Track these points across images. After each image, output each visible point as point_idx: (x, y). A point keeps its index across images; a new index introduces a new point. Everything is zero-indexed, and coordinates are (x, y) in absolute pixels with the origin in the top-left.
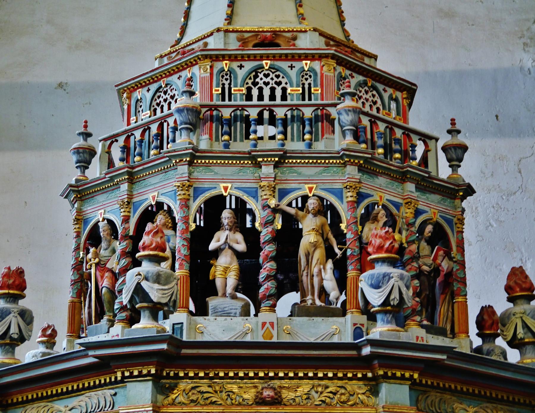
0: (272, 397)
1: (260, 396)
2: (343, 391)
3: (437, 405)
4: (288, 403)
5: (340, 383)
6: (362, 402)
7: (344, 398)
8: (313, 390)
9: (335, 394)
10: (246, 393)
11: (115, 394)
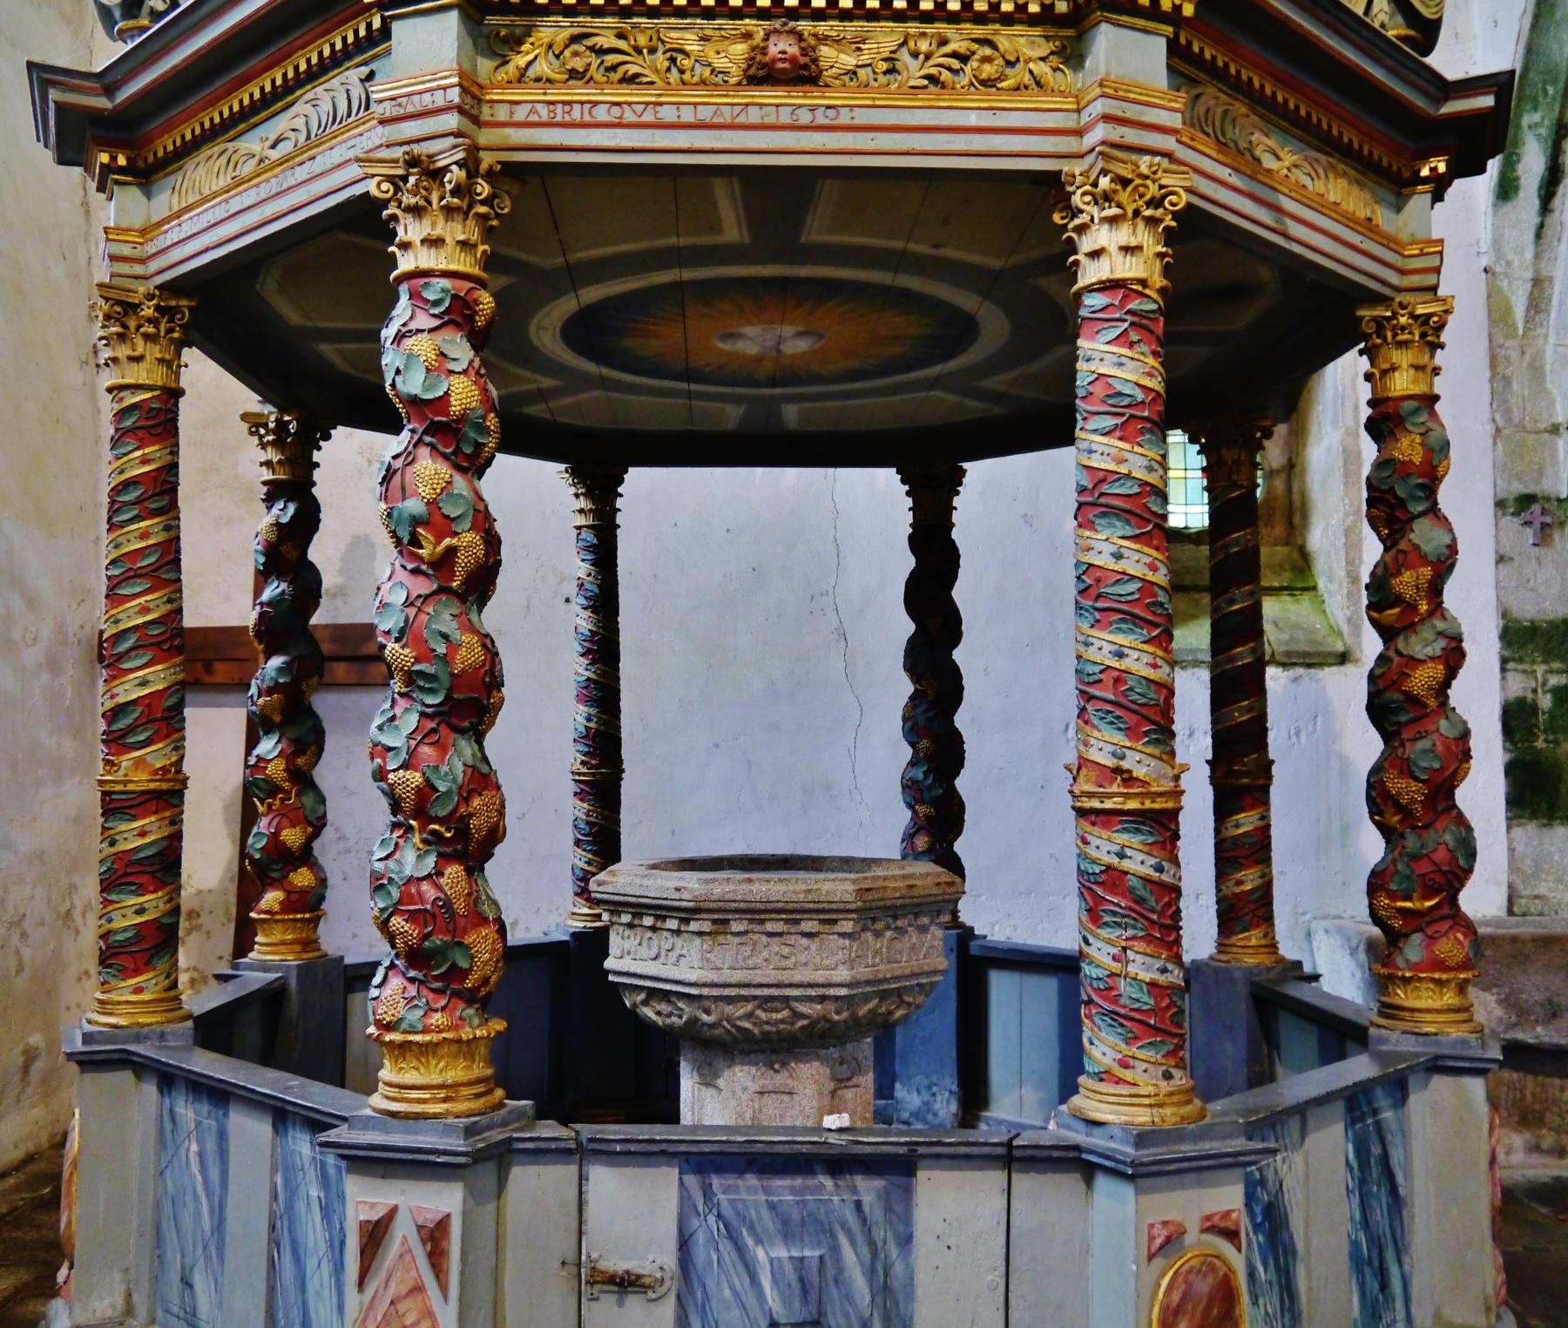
0: (793, 60)
1: (759, 57)
2: (988, 51)
3: (1218, 124)
4: (837, 82)
5: (979, 31)
6: (1038, 84)
7: (988, 70)
8: (904, 50)
9: (964, 58)
10: (722, 55)
11: (371, 76)
